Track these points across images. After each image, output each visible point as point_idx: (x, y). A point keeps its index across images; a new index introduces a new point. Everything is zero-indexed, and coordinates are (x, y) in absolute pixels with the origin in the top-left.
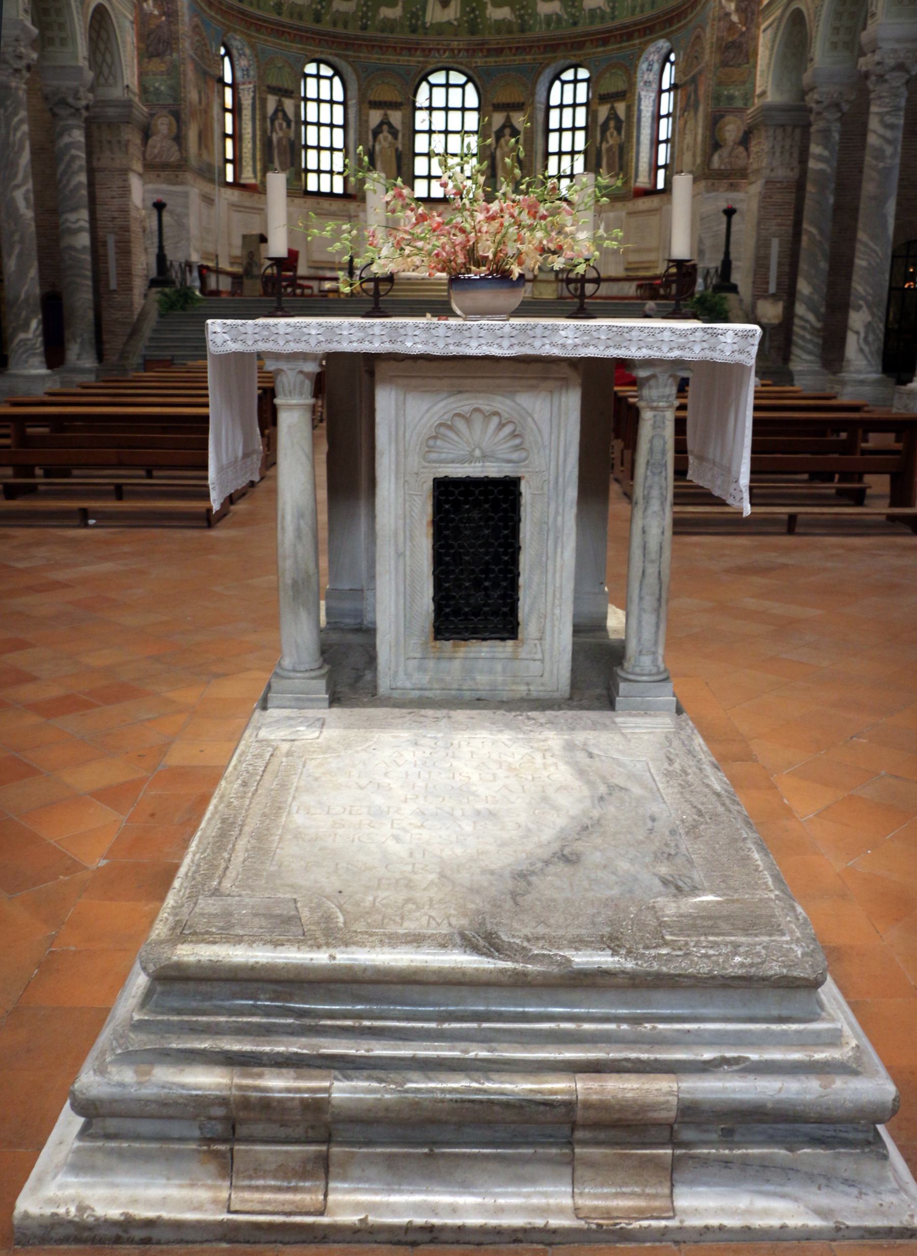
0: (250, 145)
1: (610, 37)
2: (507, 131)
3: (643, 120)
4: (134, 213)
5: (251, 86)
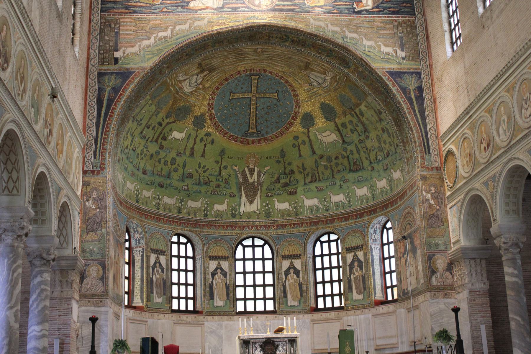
0: (139, 283)
1: (349, 216)
2: (292, 271)
3: (375, 261)
5: (141, 249)
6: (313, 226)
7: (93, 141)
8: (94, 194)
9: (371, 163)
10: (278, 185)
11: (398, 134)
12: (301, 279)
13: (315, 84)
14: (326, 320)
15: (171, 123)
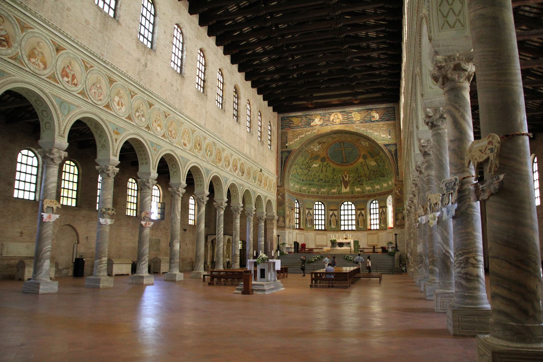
4: (274, 237)
10: (356, 182)
14: (372, 234)
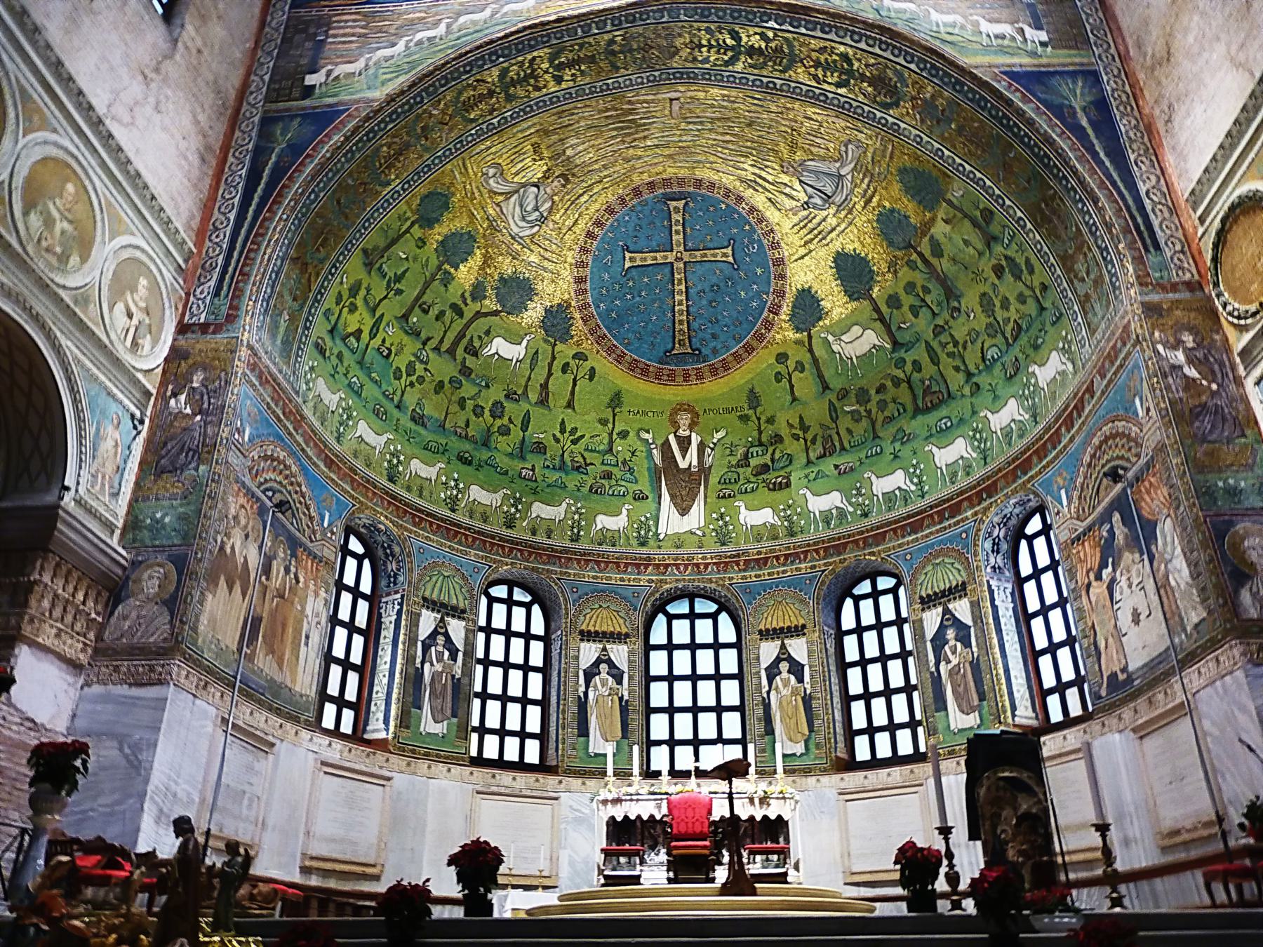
0: (385, 681)
1: (923, 519)
2: (784, 666)
3: (1003, 621)
5: (398, 596)
6: (832, 556)
7: (221, 257)
8: (195, 378)
9: (969, 375)
10: (746, 472)
11: (1045, 248)
12: (808, 686)
13: (818, 201)
15: (486, 315)
